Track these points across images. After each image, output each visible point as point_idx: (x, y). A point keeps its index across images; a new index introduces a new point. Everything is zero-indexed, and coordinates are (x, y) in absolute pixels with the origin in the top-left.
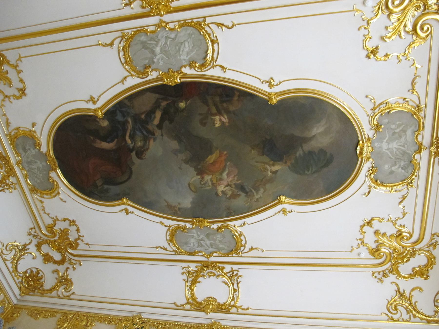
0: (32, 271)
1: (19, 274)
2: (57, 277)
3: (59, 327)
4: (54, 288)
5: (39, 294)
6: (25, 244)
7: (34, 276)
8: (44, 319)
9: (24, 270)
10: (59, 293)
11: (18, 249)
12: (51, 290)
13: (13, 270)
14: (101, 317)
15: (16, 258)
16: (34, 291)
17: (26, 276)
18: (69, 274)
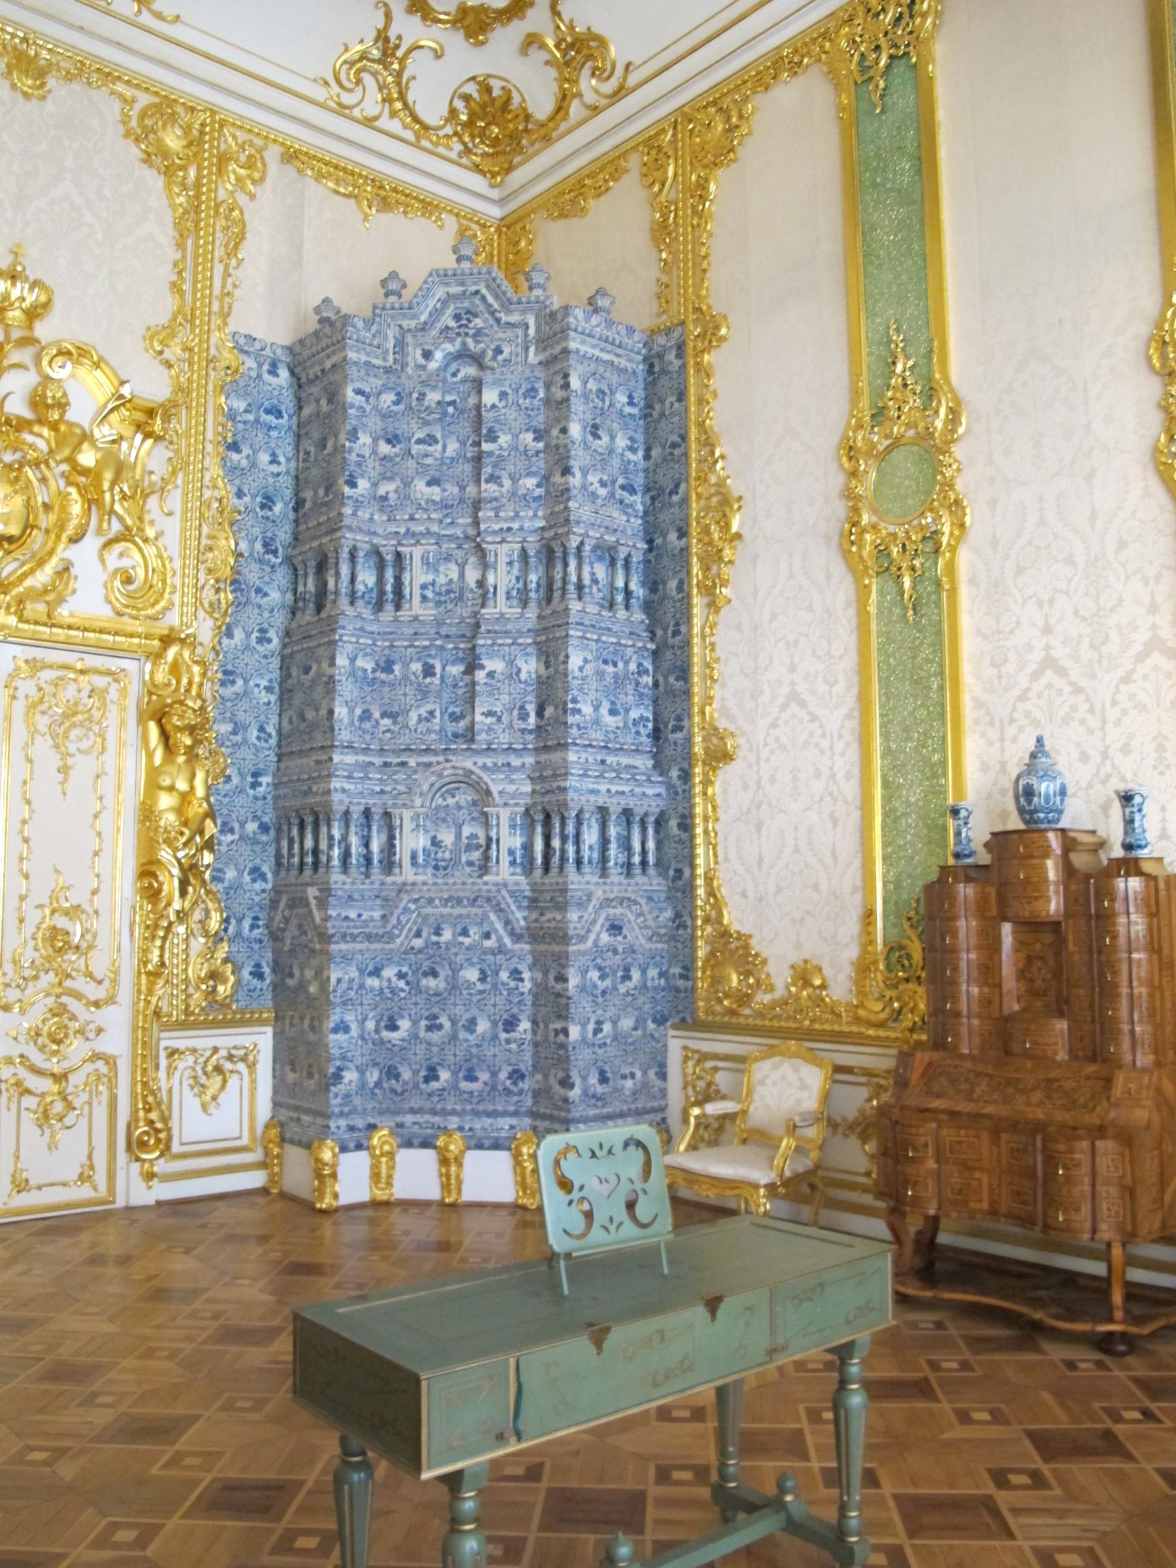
0: (467, 98)
1: (441, 133)
2: (547, 57)
3: (656, 188)
4: (564, 97)
5: (537, 146)
6: (379, 31)
7: (483, 106)
8: (603, 198)
9: (445, 112)
10: (590, 98)
11: (373, 61)
12: (559, 109)
13: (415, 132)
14: (759, 73)
15: (389, 94)
16: (519, 149)
17: (465, 125)
18: (571, 21)
